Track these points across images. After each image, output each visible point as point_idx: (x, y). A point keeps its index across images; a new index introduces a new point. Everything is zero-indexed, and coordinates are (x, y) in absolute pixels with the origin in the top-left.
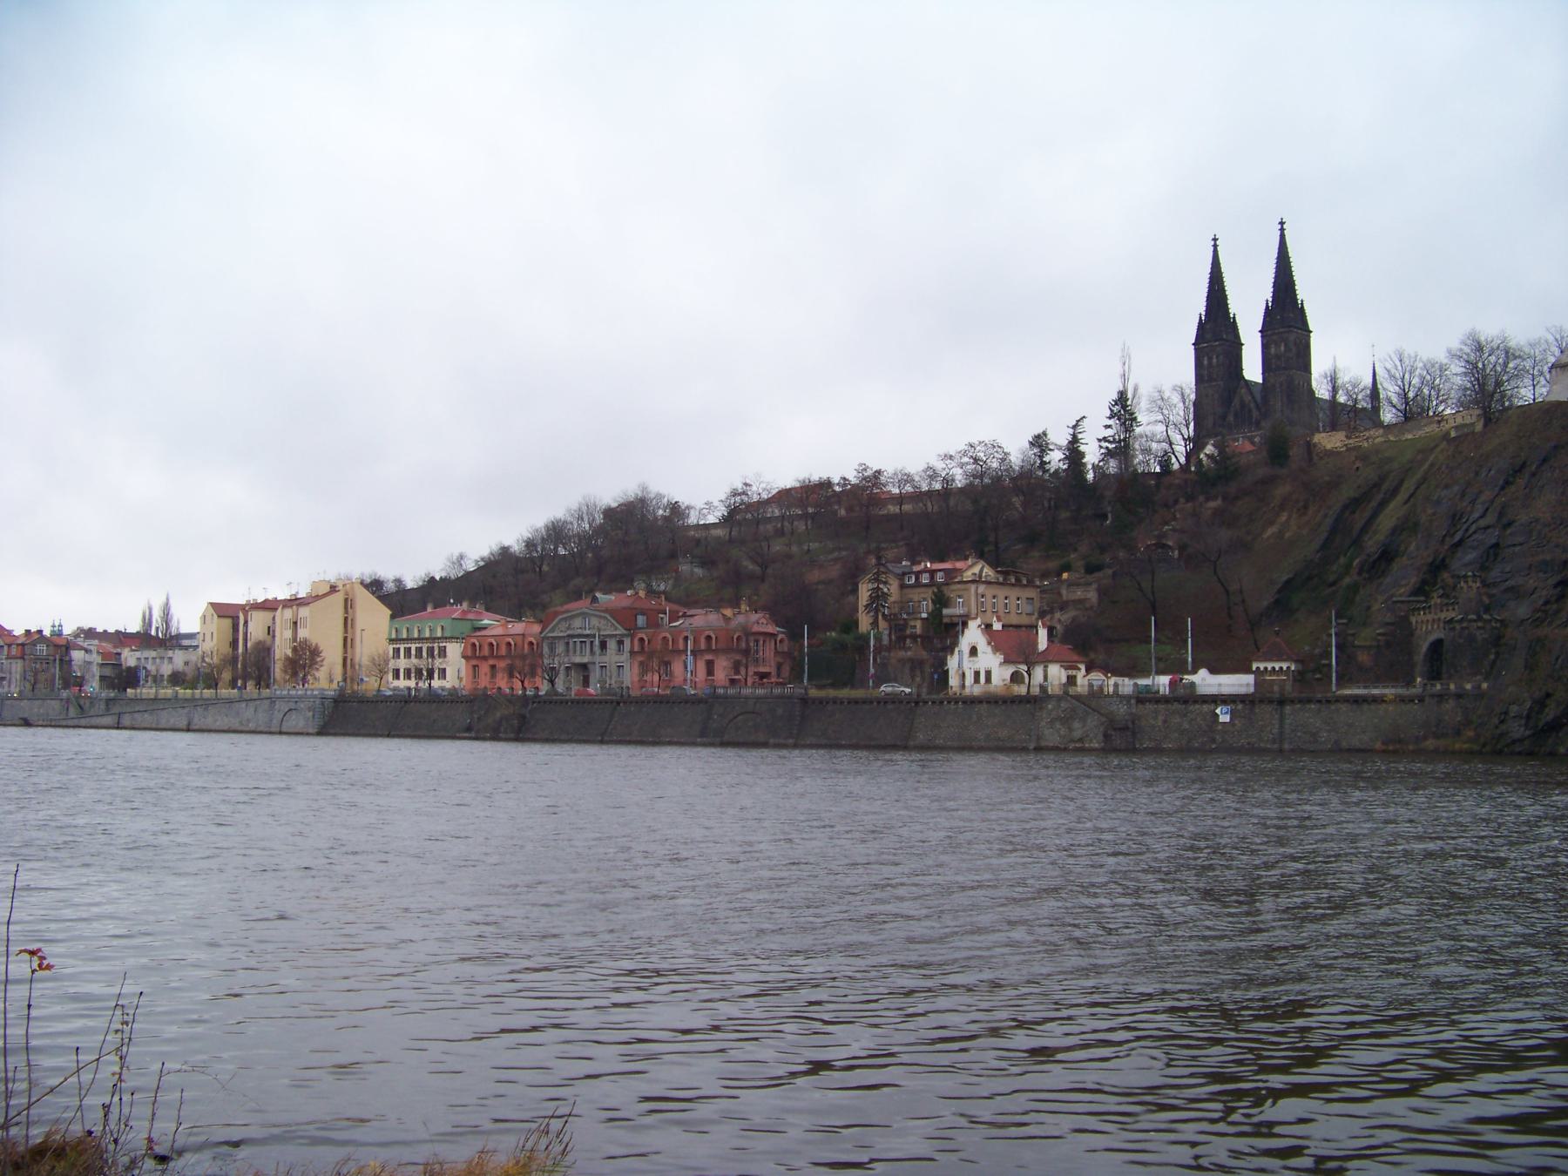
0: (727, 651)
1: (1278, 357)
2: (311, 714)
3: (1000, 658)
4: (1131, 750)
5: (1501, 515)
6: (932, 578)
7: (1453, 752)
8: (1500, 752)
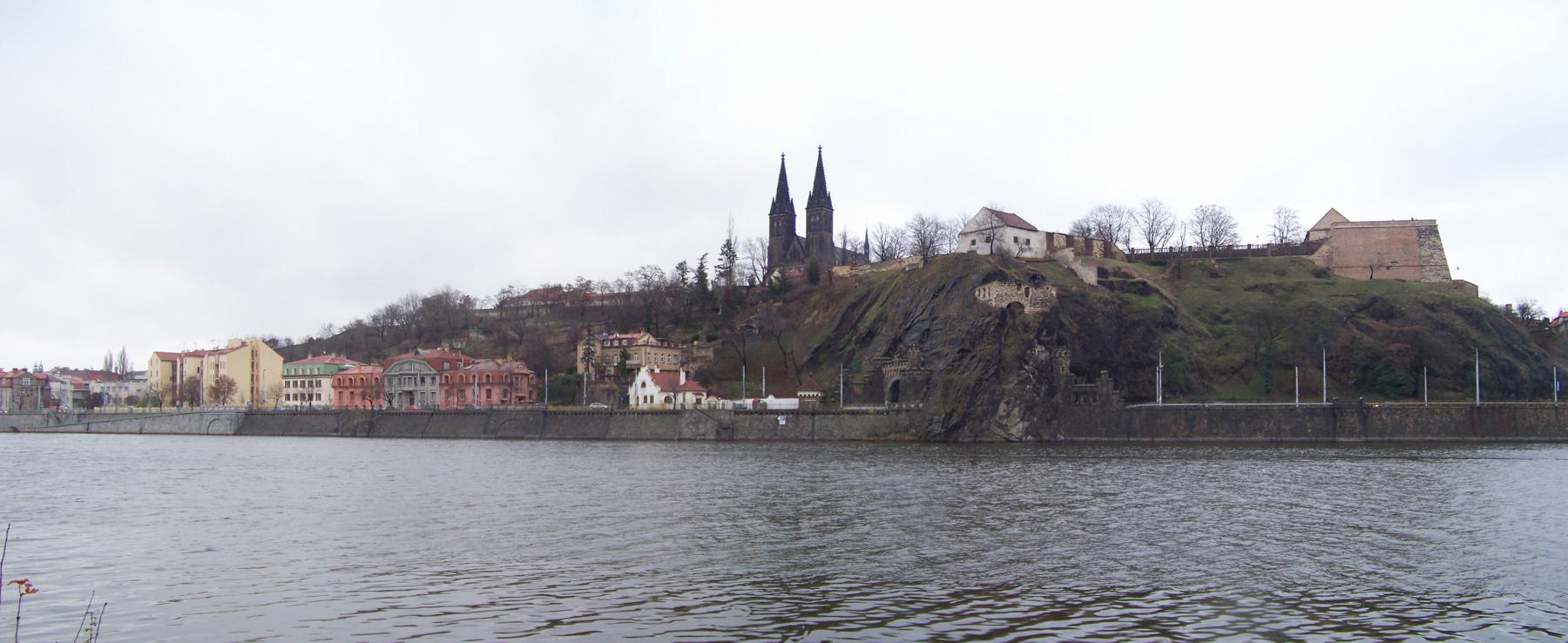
0: (499, 384)
1: (815, 223)
2: (229, 422)
3: (659, 389)
4: (731, 440)
5: (931, 314)
7: (904, 441)
8: (928, 441)
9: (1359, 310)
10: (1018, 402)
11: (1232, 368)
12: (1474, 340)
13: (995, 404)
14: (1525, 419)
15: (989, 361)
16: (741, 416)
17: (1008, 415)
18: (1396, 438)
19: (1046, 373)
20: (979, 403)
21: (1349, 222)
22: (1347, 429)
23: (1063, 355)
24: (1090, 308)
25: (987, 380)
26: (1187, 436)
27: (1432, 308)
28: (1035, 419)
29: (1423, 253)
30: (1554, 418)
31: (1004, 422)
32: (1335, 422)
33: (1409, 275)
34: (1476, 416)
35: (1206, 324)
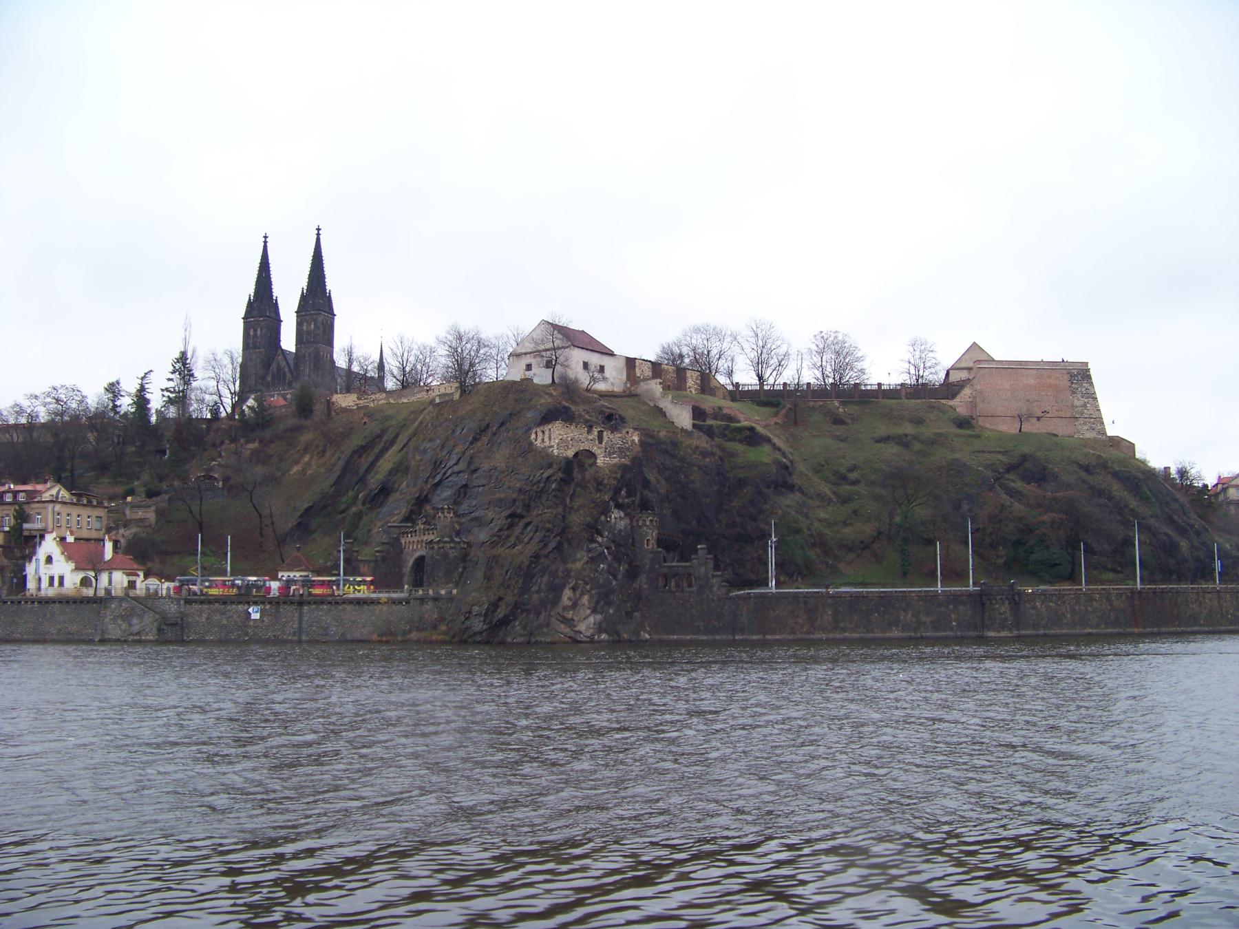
1: (308, 333)
3: (72, 565)
4: (181, 642)
5: (470, 464)
6: (15, 497)
7: (431, 642)
8: (465, 642)
9: (1008, 471)
10: (588, 587)
11: (862, 542)
12: (1132, 510)
13: (557, 590)
14: (1187, 606)
15: (548, 530)
16: (196, 606)
17: (575, 605)
18: (1052, 631)
19: (625, 546)
20: (534, 588)
21: (993, 360)
22: (998, 622)
23: (648, 523)
24: (683, 460)
25: (546, 556)
26: (807, 633)
27: (1087, 469)
28: (611, 611)
29: (1077, 403)
30: (1216, 603)
31: (570, 615)
32: (983, 612)
33: (1061, 428)
34: (1136, 602)
35: (829, 485)
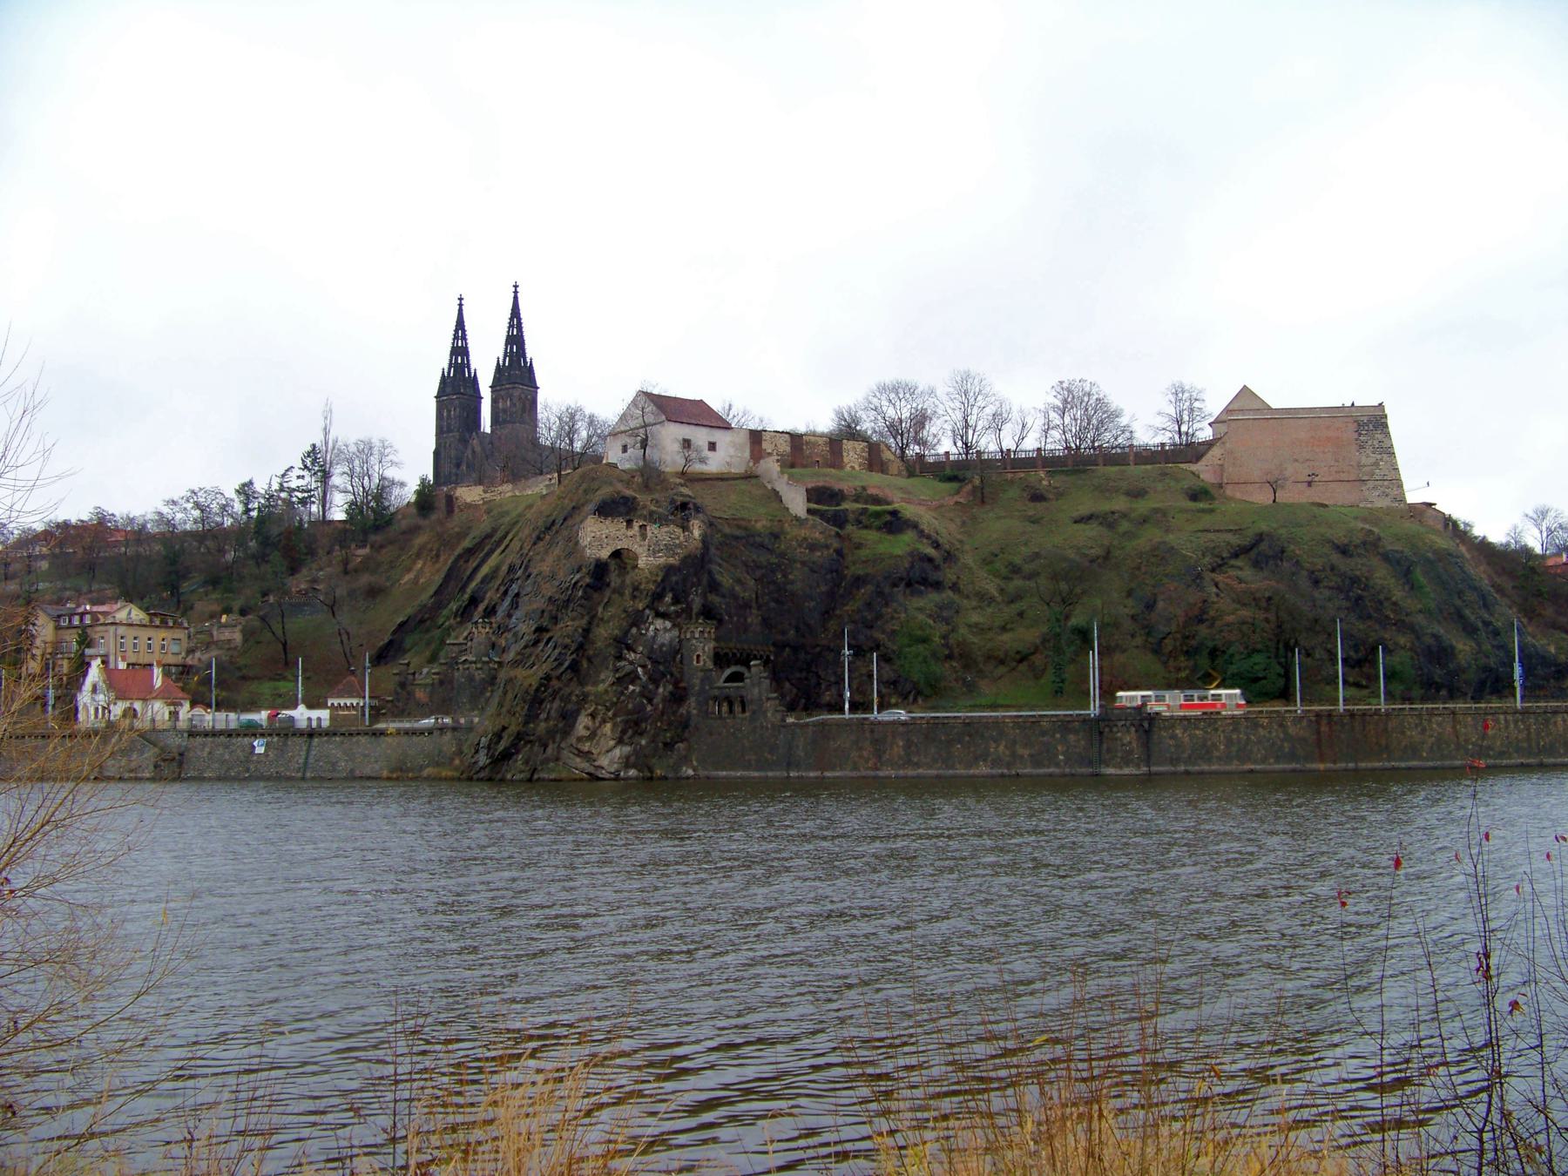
1: (505, 411)
4: (178, 779)
6: (82, 620)
7: (440, 779)
8: (470, 779)
9: (1236, 555)
10: (610, 714)
11: (1018, 652)
12: (1395, 604)
13: (569, 718)
14: (1403, 733)
15: (566, 647)
16: (199, 740)
17: (593, 735)
18: (1197, 768)
19: (667, 663)
20: (543, 716)
21: (1269, 408)
22: (1119, 754)
23: (697, 635)
24: (782, 555)
25: (559, 678)
26: (872, 769)
27: (1344, 551)
28: (643, 742)
29: (1364, 461)
30: (1449, 729)
31: (586, 747)
32: (1101, 742)
33: (1338, 496)
34: (1324, 728)
35: (997, 581)
